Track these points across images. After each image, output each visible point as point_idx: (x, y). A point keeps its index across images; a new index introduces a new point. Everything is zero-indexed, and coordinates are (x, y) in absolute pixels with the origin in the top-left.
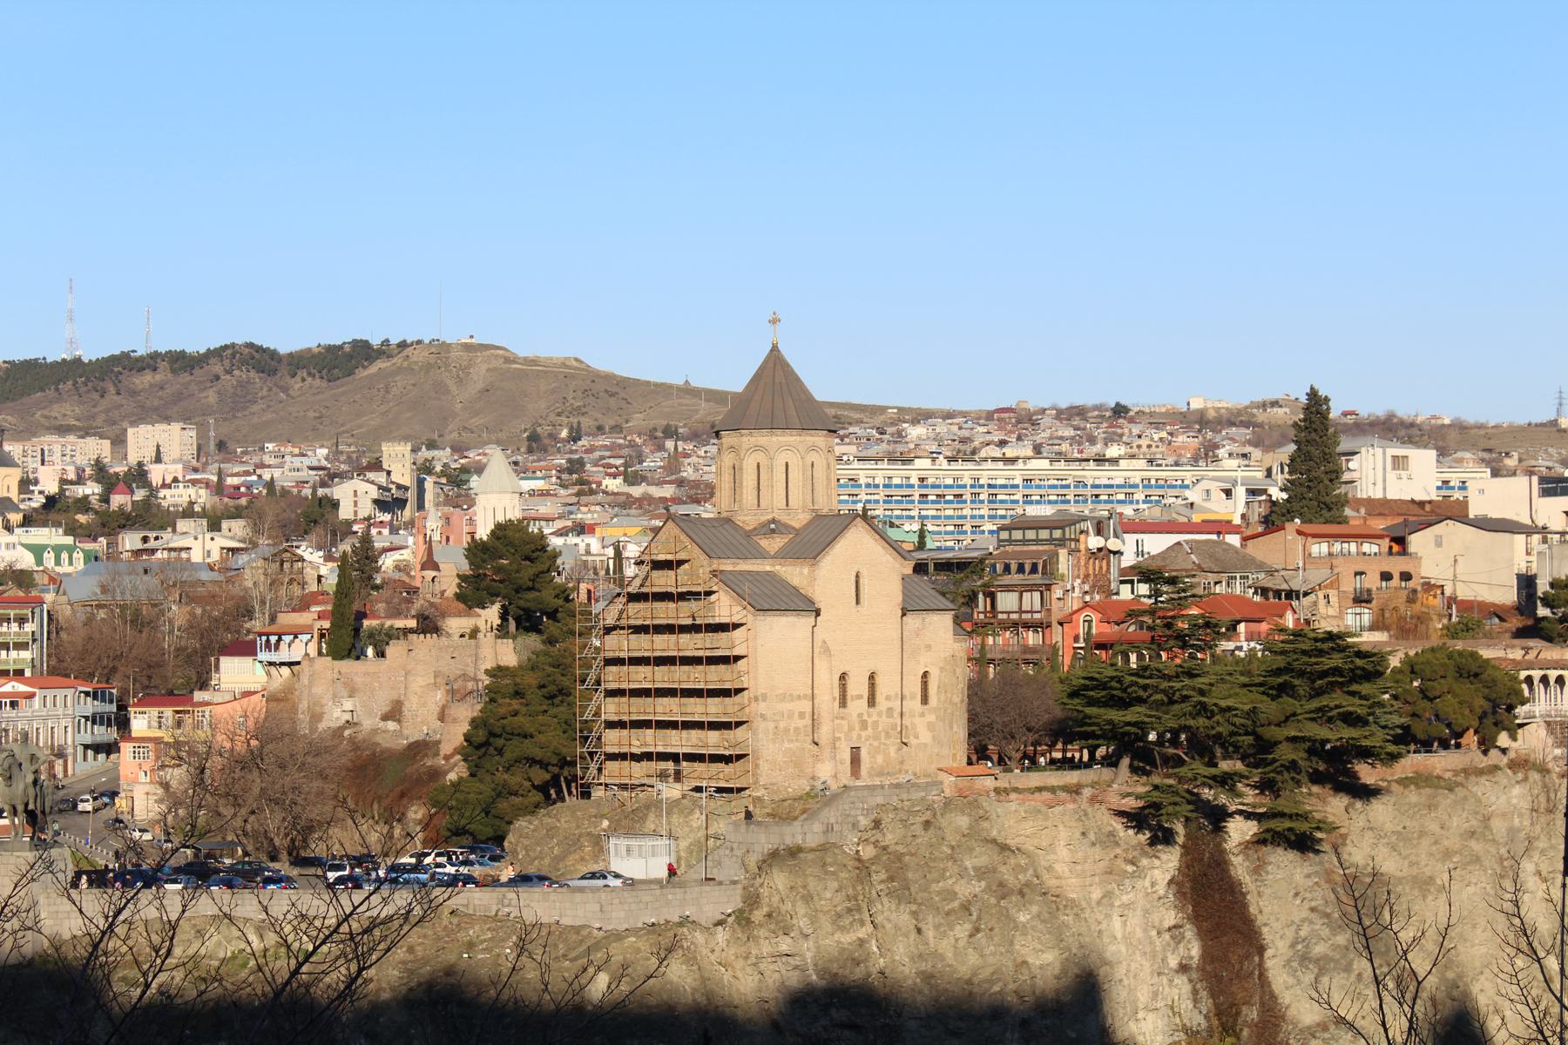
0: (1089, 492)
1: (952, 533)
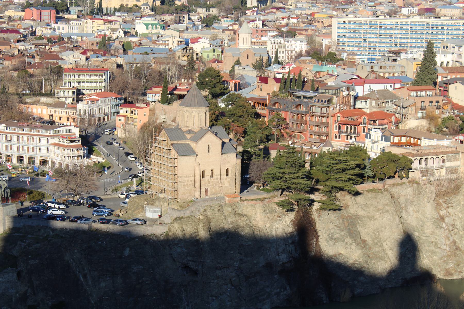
0: (431, 27)
1: (388, 38)
